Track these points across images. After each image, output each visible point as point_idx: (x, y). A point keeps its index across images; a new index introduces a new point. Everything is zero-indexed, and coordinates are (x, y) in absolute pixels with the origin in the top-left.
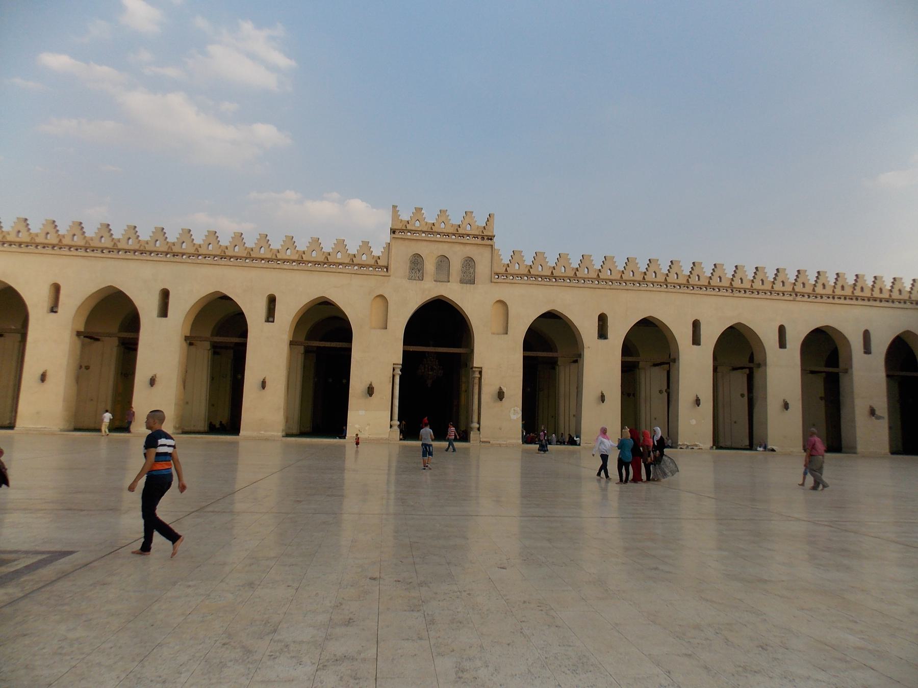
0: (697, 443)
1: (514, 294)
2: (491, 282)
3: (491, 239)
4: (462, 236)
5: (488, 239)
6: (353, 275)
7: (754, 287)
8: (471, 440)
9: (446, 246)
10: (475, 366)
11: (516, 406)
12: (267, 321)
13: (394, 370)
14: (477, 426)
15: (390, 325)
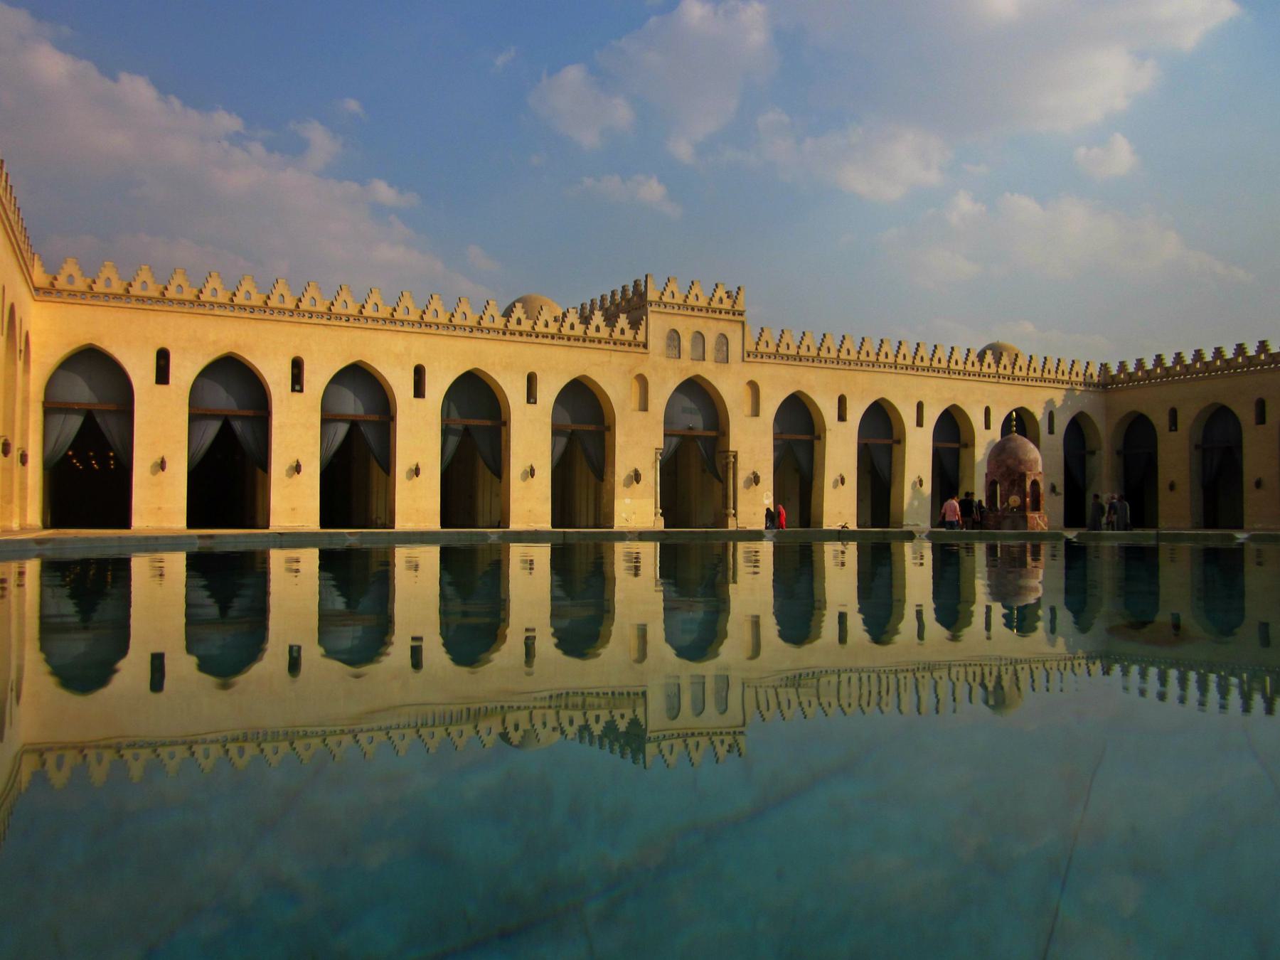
0: (919, 523)
1: (765, 373)
2: (743, 360)
3: (742, 315)
4: (714, 311)
5: (739, 314)
6: (612, 352)
7: (967, 369)
8: (729, 525)
9: (700, 321)
10: (731, 449)
11: (770, 491)
12: (528, 402)
13: (656, 453)
14: (733, 512)
15: (650, 407)
